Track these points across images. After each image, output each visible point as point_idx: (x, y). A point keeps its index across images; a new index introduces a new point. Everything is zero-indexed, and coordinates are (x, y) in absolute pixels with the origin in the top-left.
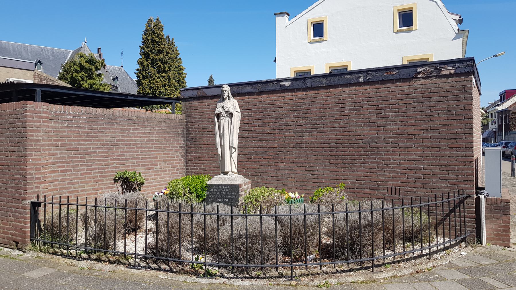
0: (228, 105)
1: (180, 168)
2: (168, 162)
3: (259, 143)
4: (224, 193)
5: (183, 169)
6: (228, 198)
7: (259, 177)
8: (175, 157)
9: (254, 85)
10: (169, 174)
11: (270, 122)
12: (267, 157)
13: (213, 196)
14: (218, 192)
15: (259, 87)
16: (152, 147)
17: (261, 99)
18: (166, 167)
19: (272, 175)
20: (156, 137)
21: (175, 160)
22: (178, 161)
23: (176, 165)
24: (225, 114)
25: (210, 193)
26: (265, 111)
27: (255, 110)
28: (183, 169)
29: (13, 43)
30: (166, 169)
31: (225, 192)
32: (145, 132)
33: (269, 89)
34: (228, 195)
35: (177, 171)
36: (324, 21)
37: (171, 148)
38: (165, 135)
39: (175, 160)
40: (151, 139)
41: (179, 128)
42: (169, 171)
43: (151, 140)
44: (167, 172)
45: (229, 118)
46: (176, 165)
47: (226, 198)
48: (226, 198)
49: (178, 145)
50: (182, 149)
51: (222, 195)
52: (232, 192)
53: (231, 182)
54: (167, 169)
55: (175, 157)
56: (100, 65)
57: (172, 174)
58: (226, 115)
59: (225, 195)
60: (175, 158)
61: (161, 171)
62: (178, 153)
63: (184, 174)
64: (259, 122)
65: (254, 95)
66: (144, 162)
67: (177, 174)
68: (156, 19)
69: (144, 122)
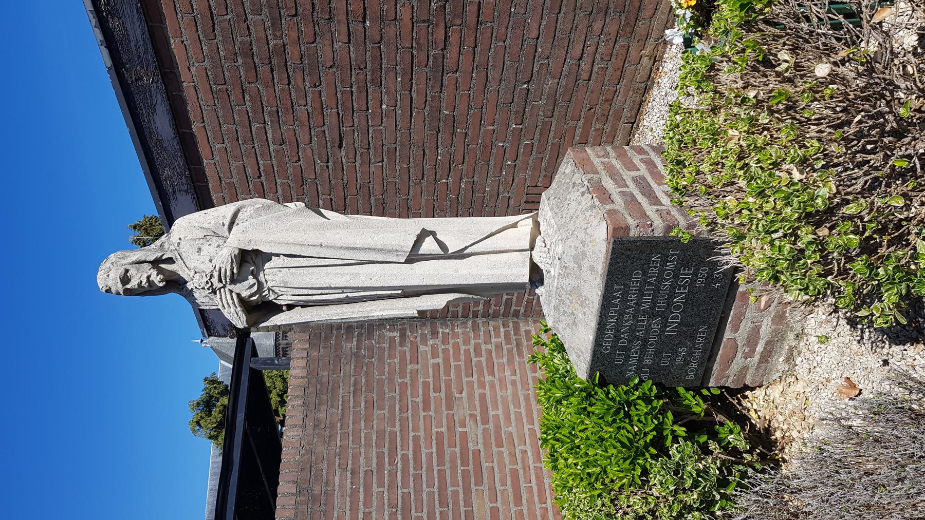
0: (203, 267)
1: (473, 342)
2: (454, 390)
3: (392, 86)
4: (645, 306)
5: (475, 328)
8: (437, 360)
9: (139, 99)
10: (493, 386)
11: (294, 35)
12: (451, 55)
13: (651, 350)
14: (632, 330)
15: (139, 78)
16: (405, 458)
17: (193, 70)
18: (471, 396)
19: (534, 34)
20: (368, 445)
21: (446, 360)
22: (450, 347)
23: (462, 357)
24: (246, 284)
25: (633, 361)
26: (249, 53)
27: (247, 97)
28: (475, 328)
29: (213, 457)
30: (477, 397)
31: (638, 304)
32: (349, 491)
33: (139, 34)
34: (657, 291)
35: (484, 353)
37: (408, 380)
38: (363, 404)
39: (446, 360)
40: (374, 465)
41: (338, 346)
42: (482, 385)
43: (380, 465)
44: (488, 392)
45: (267, 265)
46: (462, 357)
47: (671, 296)
48: (671, 296)
49: (398, 353)
50: (408, 333)
51: (651, 314)
52: (644, 273)
54: (477, 392)
55: (437, 360)
56: (215, 388)
57: (493, 374)
58: (251, 280)
59: (654, 303)
60: (440, 360)
61: (485, 421)
62: (422, 348)
63: (492, 323)
64: (300, 83)
65: (184, 103)
66: (455, 493)
67: (494, 354)
68: (133, 230)
69: (315, 499)
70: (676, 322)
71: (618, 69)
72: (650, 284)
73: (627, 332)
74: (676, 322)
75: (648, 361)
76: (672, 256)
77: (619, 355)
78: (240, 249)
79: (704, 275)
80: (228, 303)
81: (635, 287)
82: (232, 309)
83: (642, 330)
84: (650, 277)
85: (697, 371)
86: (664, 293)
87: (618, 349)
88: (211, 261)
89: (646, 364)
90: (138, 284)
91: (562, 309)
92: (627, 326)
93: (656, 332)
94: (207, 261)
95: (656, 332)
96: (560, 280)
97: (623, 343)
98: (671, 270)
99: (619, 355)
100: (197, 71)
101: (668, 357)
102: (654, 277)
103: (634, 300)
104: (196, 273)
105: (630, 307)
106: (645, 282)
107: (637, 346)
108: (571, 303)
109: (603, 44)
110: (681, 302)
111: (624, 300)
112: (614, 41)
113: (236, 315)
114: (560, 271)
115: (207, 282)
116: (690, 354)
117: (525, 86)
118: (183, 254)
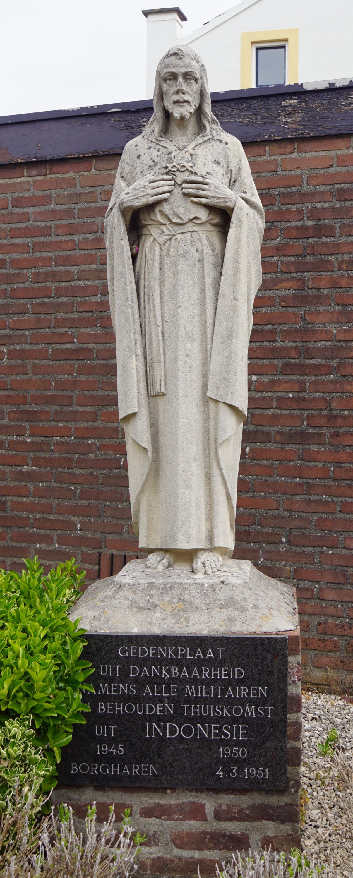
4: (190, 691)
6: (219, 720)
7: (283, 548)
13: (121, 708)
31: (195, 681)
34: (216, 701)
36: (287, 40)
47: (203, 720)
48: (203, 720)
51: (176, 702)
52: (240, 682)
53: (231, 620)
59: (196, 701)
70: (165, 734)
71: (307, 645)
72: (224, 692)
73: (150, 674)
74: (165, 734)
75: (102, 708)
76: (264, 711)
77: (114, 669)
78: (232, 210)
79: (235, 754)
80: (158, 187)
81: (221, 672)
82: (150, 191)
84: (234, 690)
85: (85, 775)
86: (210, 711)
87: (123, 666)
88: (208, 173)
90: (182, 90)
91: (153, 592)
92: (161, 673)
93: (151, 709)
94: (207, 170)
95: (151, 709)
96: (194, 587)
97: (133, 671)
98: (244, 713)
100: (296, 176)
101: (109, 733)
102: (235, 694)
103: (201, 675)
104: (191, 155)
106: (227, 683)
107: (129, 690)
108: (169, 602)
109: (337, 622)
110: (196, 734)
111: (200, 663)
112: (342, 634)
113: (142, 194)
114: (206, 585)
115: (184, 166)
116: (110, 759)
117: (284, 540)
118: (210, 145)
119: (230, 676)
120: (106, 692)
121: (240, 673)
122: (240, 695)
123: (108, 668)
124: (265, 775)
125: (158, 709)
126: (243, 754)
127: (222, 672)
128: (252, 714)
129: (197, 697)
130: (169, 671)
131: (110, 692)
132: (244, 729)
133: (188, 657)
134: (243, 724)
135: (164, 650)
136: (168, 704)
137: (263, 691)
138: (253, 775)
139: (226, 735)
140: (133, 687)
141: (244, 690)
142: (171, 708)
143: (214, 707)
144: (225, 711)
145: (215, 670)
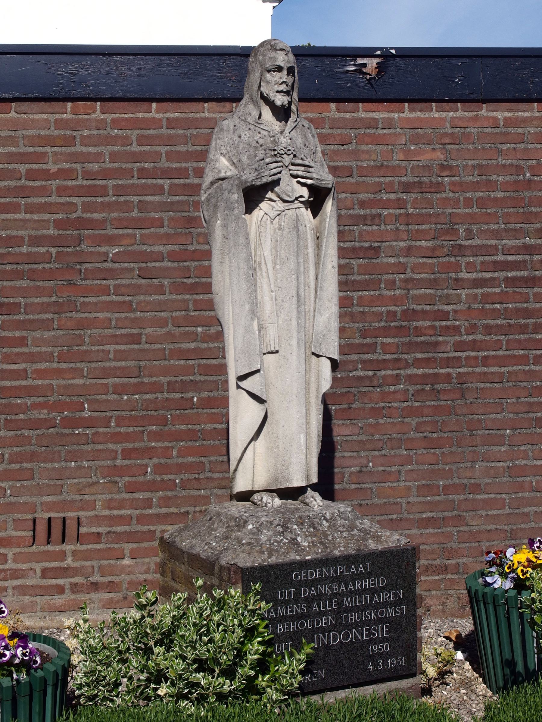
4: (347, 602)
6: (369, 623)
14: (318, 598)
31: (350, 594)
34: (365, 608)
47: (356, 625)
48: (356, 625)
51: (337, 613)
52: (383, 589)
59: (351, 610)
70: (329, 642)
72: (372, 598)
73: (317, 593)
77: (290, 593)
79: (381, 649)
81: (369, 583)
83: (319, 607)
84: (379, 596)
86: (362, 617)
87: (296, 589)
89: (277, 628)
92: (325, 590)
93: (318, 623)
95: (318, 623)
99: (290, 593)
102: (380, 599)
105: (346, 585)
106: (374, 591)
107: (301, 609)
110: (352, 638)
111: (354, 578)
119: (375, 585)
120: (283, 614)
121: (383, 581)
122: (383, 599)
123: (285, 593)
124: (402, 662)
125: (324, 621)
126: (386, 649)
127: (369, 583)
128: (392, 614)
129: (352, 607)
130: (331, 588)
131: (286, 613)
132: (387, 627)
133: (345, 574)
134: (386, 623)
135: (327, 571)
136: (331, 616)
137: (400, 593)
138: (394, 664)
139: (374, 635)
140: (304, 606)
141: (386, 595)
142: (333, 619)
143: (365, 614)
144: (373, 615)
145: (365, 582)
